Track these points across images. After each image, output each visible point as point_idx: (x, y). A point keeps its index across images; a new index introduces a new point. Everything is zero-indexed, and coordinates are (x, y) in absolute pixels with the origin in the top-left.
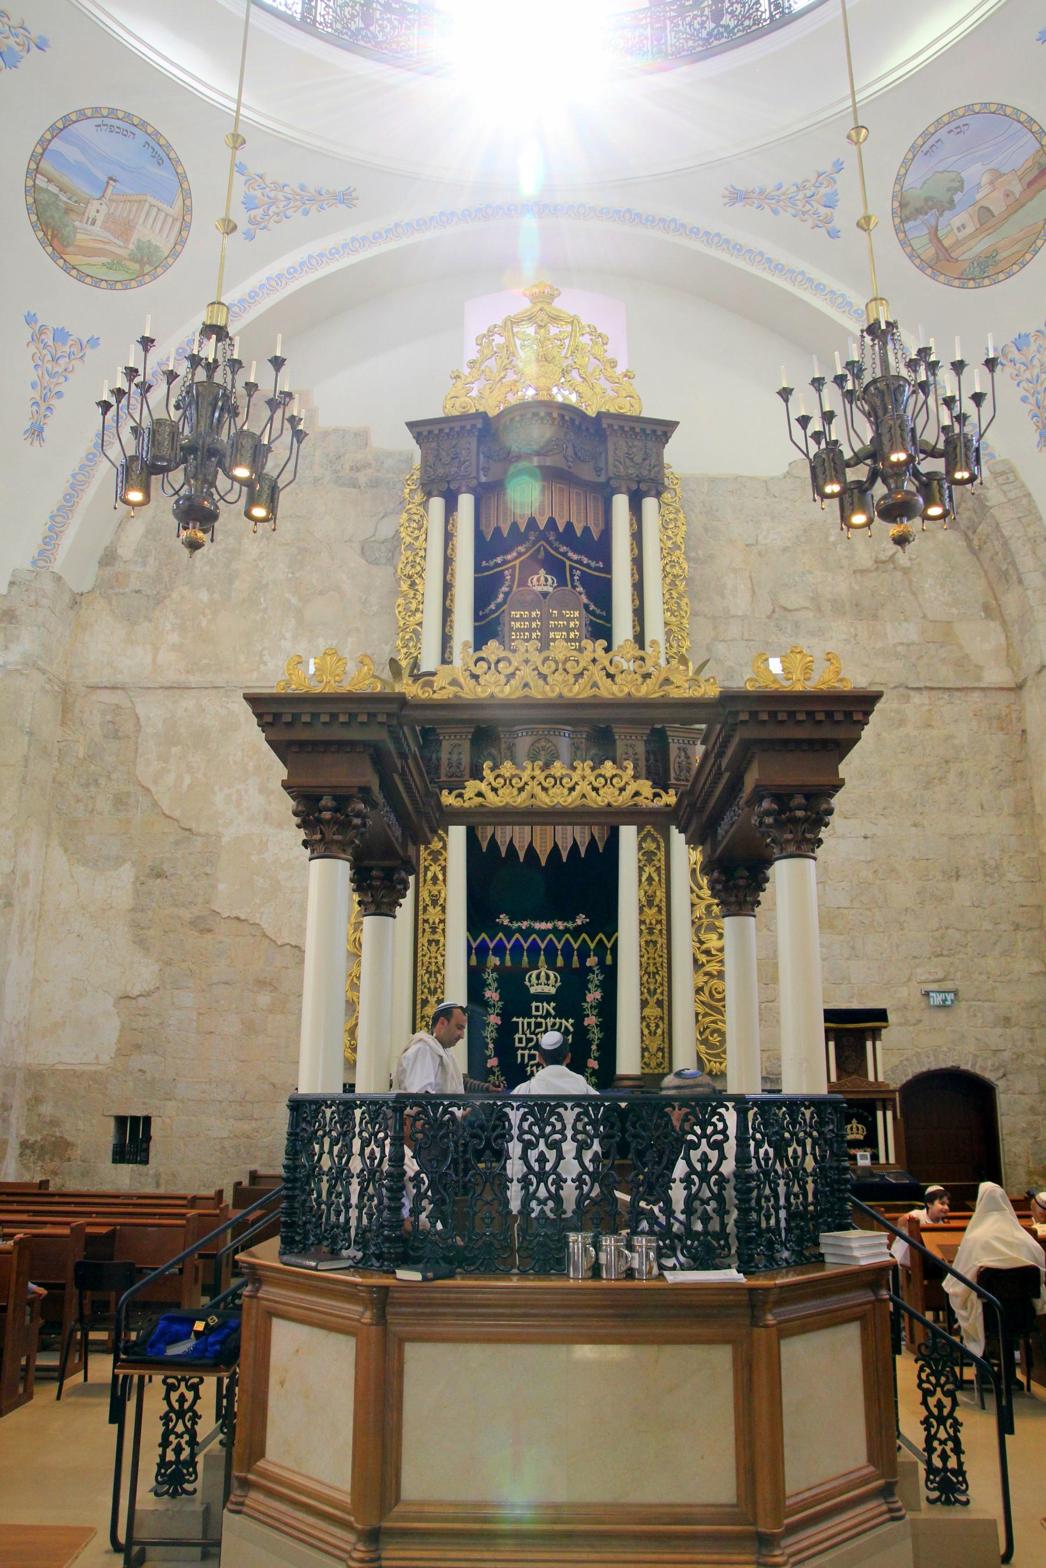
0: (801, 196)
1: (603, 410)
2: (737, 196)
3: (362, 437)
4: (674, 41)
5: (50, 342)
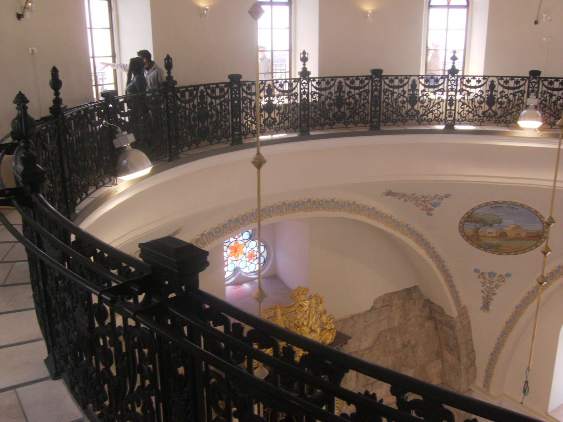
0: (423, 199)
2: (390, 193)
4: (385, 110)
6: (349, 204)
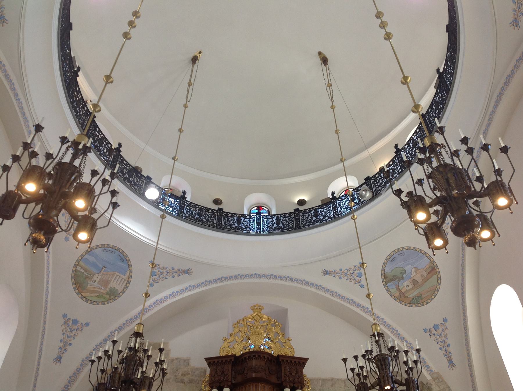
0: (349, 273)
1: (280, 354)
2: (326, 273)
3: (187, 361)
5: (70, 324)
6: (300, 280)
